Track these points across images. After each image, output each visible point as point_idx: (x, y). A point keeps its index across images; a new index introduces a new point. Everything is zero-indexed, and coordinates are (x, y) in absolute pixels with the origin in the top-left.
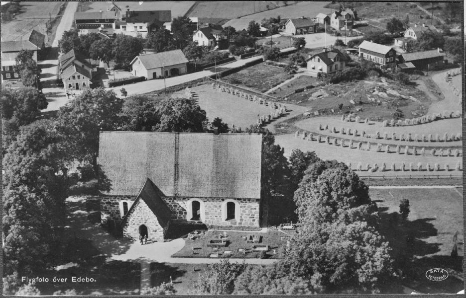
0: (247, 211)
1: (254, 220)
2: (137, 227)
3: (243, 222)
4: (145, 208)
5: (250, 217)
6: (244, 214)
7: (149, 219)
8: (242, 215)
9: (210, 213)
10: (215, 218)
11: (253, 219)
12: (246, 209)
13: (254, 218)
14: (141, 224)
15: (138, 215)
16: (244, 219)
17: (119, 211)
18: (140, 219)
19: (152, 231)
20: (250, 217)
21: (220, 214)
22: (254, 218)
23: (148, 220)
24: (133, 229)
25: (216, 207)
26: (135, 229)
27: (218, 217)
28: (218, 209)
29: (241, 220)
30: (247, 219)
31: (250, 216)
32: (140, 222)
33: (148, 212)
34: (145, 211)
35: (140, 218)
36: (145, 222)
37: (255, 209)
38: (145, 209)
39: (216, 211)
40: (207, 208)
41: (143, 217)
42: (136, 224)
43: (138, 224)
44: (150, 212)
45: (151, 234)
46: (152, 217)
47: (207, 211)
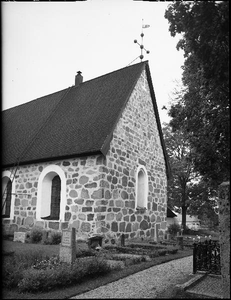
0: (79, 191)
1: (91, 217)
3: (71, 222)
5: (84, 210)
6: (73, 199)
8: (69, 201)
9: (21, 200)
10: (27, 211)
11: (89, 213)
12: (77, 187)
13: (90, 209)
16: (73, 214)
20: (84, 210)
21: (34, 202)
22: (90, 209)
25: (30, 185)
27: (32, 209)
28: (33, 190)
29: (68, 216)
30: (78, 213)
31: (84, 205)
37: (95, 185)
39: (29, 196)
47: (18, 197)
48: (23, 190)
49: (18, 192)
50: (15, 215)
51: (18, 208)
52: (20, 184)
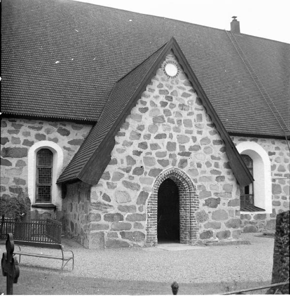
2: (151, 186)
4: (186, 101)
7: (196, 148)
14: (166, 171)
15: (161, 130)
17: (24, 182)
18: (163, 149)
19: (202, 201)
23: (193, 153)
24: (134, 195)
26: (144, 195)
32: (164, 163)
33: (193, 118)
34: (184, 113)
35: (163, 144)
36: (183, 163)
38: (182, 106)
40: (276, 171)
41: (175, 140)
42: (147, 169)
43: (154, 172)
44: (199, 117)
45: (202, 217)
46: (205, 140)
47: (277, 182)
48: (283, 173)
49: (276, 175)
50: (274, 207)
51: (278, 197)
52: (278, 165)
